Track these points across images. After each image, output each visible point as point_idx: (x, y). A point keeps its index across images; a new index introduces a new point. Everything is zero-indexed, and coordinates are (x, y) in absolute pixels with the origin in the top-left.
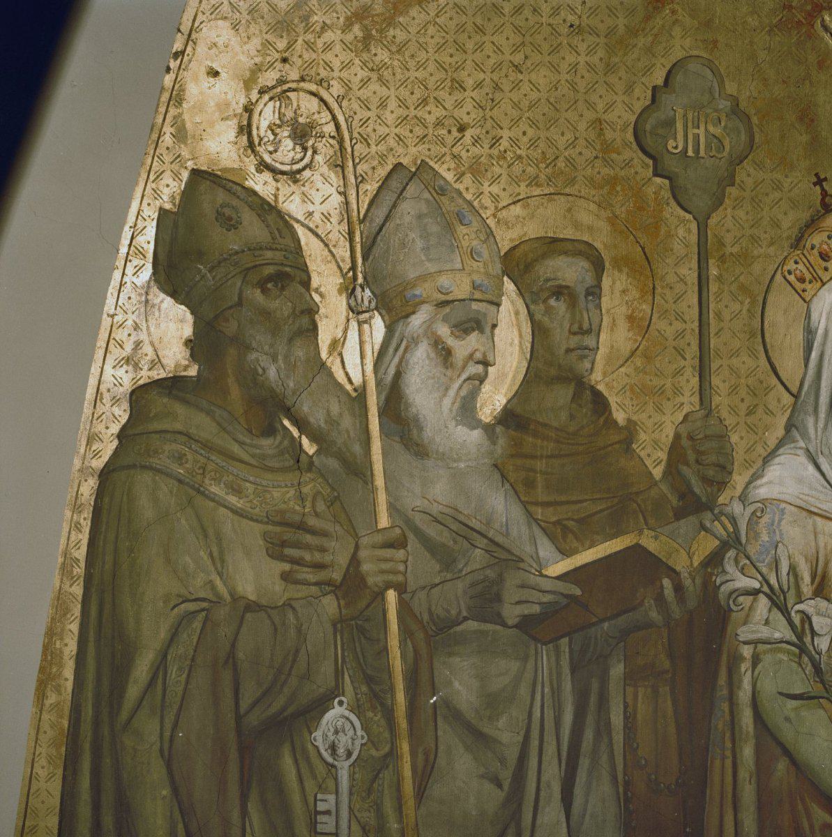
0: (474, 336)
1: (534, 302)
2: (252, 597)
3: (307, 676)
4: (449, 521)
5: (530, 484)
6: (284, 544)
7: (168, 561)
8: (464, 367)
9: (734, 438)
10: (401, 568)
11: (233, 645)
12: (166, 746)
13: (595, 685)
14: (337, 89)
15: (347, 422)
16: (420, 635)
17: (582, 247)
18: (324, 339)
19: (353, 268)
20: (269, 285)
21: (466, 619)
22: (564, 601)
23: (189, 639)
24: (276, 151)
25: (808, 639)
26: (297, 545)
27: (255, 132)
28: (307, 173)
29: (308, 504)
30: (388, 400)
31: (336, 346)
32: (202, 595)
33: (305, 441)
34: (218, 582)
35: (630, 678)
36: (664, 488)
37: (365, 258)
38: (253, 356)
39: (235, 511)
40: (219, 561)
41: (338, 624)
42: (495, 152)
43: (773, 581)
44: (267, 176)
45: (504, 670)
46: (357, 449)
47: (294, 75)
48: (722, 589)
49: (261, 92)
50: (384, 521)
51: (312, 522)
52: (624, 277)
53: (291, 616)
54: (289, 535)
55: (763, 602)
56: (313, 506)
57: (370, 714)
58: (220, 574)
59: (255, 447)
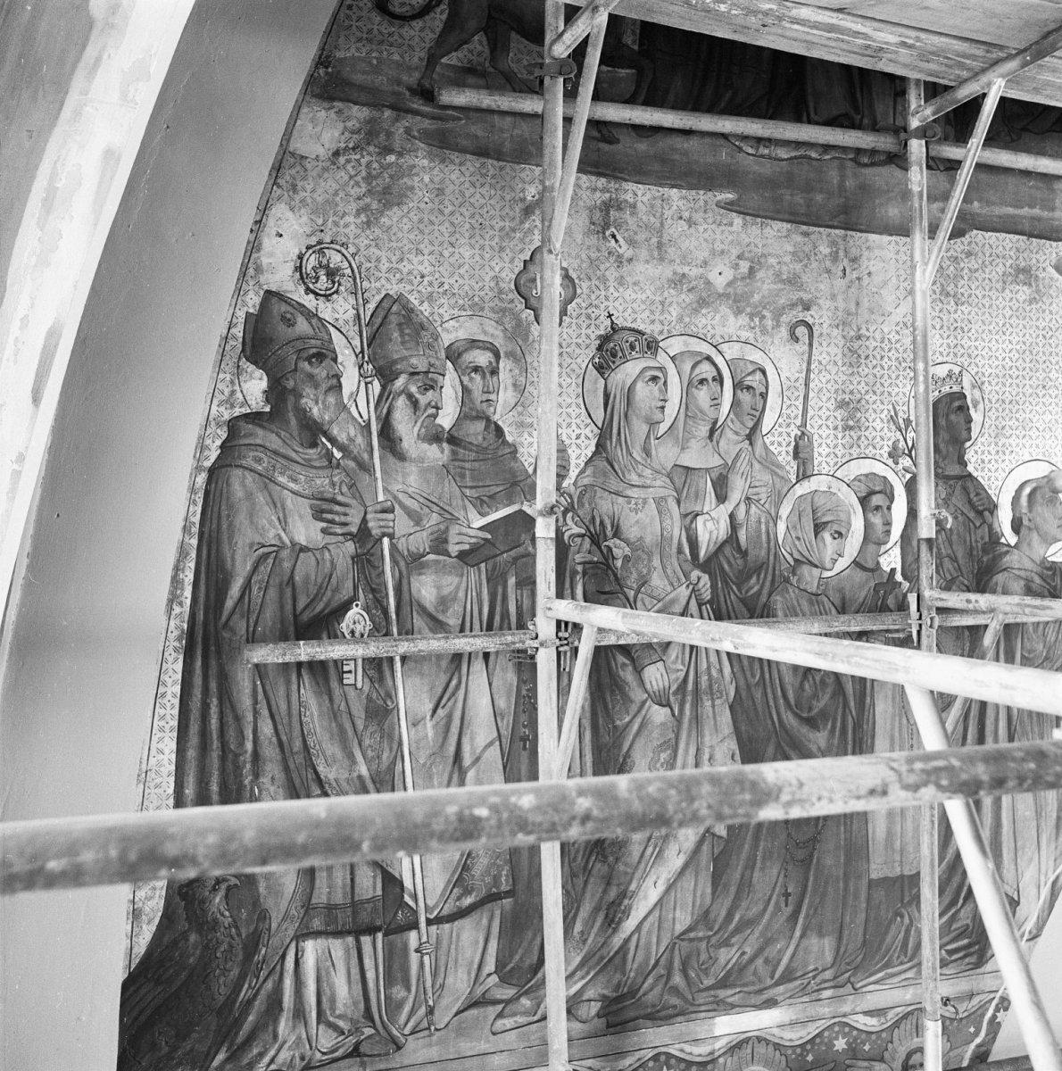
0: (431, 393)
1: (463, 374)
2: (304, 543)
3: (336, 590)
4: (417, 497)
5: (463, 476)
6: (323, 511)
7: (252, 522)
8: (425, 410)
9: (570, 451)
10: (391, 524)
11: (292, 572)
12: (250, 635)
13: (500, 590)
14: (352, 249)
15: (359, 440)
16: (402, 564)
17: (489, 346)
18: (346, 391)
19: (362, 352)
20: (314, 360)
21: (428, 553)
22: (483, 542)
24: (316, 282)
25: (610, 561)
26: (331, 512)
27: (304, 270)
28: (335, 296)
29: (337, 487)
30: (382, 428)
31: (354, 396)
32: (273, 542)
33: (335, 451)
34: (283, 534)
37: (369, 346)
38: (304, 401)
39: (293, 492)
40: (283, 522)
41: (356, 558)
42: (441, 290)
43: (592, 530)
44: (311, 296)
45: (450, 582)
46: (366, 456)
47: (328, 240)
49: (308, 248)
50: (381, 498)
51: (340, 498)
52: (510, 362)
53: (327, 554)
54: (325, 506)
55: (587, 540)
56: (340, 489)
57: (374, 611)
58: (284, 530)
59: (306, 454)
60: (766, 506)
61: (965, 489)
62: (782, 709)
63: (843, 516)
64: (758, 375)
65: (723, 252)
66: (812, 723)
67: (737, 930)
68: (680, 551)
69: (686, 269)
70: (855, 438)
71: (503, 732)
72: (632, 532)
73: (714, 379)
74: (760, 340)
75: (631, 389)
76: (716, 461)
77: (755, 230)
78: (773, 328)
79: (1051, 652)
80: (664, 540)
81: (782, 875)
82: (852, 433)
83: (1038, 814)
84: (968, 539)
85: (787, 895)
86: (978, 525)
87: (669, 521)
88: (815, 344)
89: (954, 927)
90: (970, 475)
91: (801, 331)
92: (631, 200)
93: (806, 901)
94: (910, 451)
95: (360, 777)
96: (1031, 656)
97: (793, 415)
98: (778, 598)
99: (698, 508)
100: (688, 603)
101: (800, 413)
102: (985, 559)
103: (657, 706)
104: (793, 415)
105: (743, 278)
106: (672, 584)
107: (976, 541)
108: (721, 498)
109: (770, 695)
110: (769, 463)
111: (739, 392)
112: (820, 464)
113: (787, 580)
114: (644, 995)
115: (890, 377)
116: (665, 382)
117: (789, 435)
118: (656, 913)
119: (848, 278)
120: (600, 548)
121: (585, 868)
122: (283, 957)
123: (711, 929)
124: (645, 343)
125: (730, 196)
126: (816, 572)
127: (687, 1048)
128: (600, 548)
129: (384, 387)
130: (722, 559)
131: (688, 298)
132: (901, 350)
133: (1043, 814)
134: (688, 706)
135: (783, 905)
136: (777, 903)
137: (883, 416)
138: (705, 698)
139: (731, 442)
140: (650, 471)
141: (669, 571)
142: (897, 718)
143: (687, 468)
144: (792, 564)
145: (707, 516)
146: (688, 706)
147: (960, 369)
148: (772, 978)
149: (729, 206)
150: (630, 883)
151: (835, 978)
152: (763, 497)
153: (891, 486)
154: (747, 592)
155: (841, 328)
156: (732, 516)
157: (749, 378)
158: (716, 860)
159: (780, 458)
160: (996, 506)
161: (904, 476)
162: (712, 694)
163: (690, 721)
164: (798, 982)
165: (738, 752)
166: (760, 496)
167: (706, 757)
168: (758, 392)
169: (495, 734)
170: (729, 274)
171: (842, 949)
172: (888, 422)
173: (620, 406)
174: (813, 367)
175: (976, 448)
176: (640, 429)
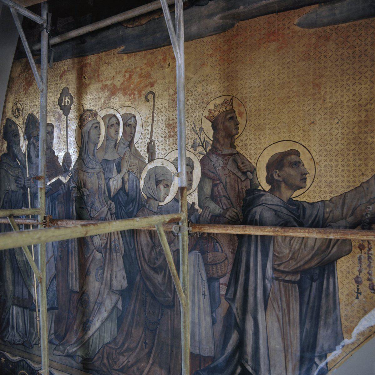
9: (72, 157)
14: (22, 102)
18: (21, 145)
23: (6, 197)
31: (22, 145)
33: (19, 162)
35: (58, 203)
36: (62, 167)
43: (77, 184)
47: (17, 101)
50: (28, 176)
60: (136, 174)
61: (235, 161)
62: (143, 262)
63: (169, 177)
64: (133, 119)
65: (120, 72)
67: (127, 350)
68: (104, 193)
69: (106, 83)
70: (175, 140)
71: (55, 254)
72: (89, 186)
73: (116, 124)
74: (133, 104)
75: (89, 132)
76: (116, 157)
77: (132, 59)
78: (138, 98)
79: (296, 256)
80: (99, 188)
81: (143, 335)
82: (173, 138)
84: (237, 188)
85: (146, 344)
86: (243, 179)
87: (101, 181)
88: (156, 100)
90: (238, 153)
91: (150, 96)
92: (90, 62)
93: (154, 349)
94: (203, 144)
95: (24, 260)
96: (281, 255)
97: (147, 134)
98: (140, 213)
99: (110, 176)
100: (107, 213)
101: (150, 132)
102: (248, 198)
103: (97, 252)
104: (147, 134)
105: (127, 80)
106: (102, 205)
107: (242, 189)
108: (119, 172)
109: (137, 255)
110: (137, 155)
111: (125, 127)
112: (158, 154)
113: (144, 206)
114: (95, 362)
115: (192, 109)
116: (100, 128)
117: (145, 142)
118: (98, 332)
119: (171, 67)
120: (80, 191)
121: (77, 306)
122: (10, 309)
123: (117, 346)
124: (93, 114)
125: (122, 48)
126: (156, 202)
128: (80, 191)
129: (28, 142)
130: (119, 196)
131: (107, 94)
132: (197, 95)
133: (290, 351)
134: (108, 254)
136: (142, 346)
137: (188, 128)
138: (113, 252)
139: (122, 148)
140: (95, 162)
141: (101, 201)
142: (196, 277)
143: (107, 160)
144: (146, 198)
145: (114, 179)
146: (108, 254)
147: (231, 97)
149: (123, 52)
150: (90, 318)
152: (135, 170)
153: (193, 162)
154: (128, 210)
155: (167, 91)
156: (123, 179)
157: (129, 121)
158: (118, 318)
159: (141, 153)
160: (255, 169)
161: (199, 156)
162: (116, 250)
163: (108, 261)
165: (125, 276)
166: (133, 170)
167: (114, 276)
168: (132, 126)
170: (122, 80)
172: (191, 131)
173: (86, 139)
174: (155, 111)
175: (242, 138)
176: (91, 146)
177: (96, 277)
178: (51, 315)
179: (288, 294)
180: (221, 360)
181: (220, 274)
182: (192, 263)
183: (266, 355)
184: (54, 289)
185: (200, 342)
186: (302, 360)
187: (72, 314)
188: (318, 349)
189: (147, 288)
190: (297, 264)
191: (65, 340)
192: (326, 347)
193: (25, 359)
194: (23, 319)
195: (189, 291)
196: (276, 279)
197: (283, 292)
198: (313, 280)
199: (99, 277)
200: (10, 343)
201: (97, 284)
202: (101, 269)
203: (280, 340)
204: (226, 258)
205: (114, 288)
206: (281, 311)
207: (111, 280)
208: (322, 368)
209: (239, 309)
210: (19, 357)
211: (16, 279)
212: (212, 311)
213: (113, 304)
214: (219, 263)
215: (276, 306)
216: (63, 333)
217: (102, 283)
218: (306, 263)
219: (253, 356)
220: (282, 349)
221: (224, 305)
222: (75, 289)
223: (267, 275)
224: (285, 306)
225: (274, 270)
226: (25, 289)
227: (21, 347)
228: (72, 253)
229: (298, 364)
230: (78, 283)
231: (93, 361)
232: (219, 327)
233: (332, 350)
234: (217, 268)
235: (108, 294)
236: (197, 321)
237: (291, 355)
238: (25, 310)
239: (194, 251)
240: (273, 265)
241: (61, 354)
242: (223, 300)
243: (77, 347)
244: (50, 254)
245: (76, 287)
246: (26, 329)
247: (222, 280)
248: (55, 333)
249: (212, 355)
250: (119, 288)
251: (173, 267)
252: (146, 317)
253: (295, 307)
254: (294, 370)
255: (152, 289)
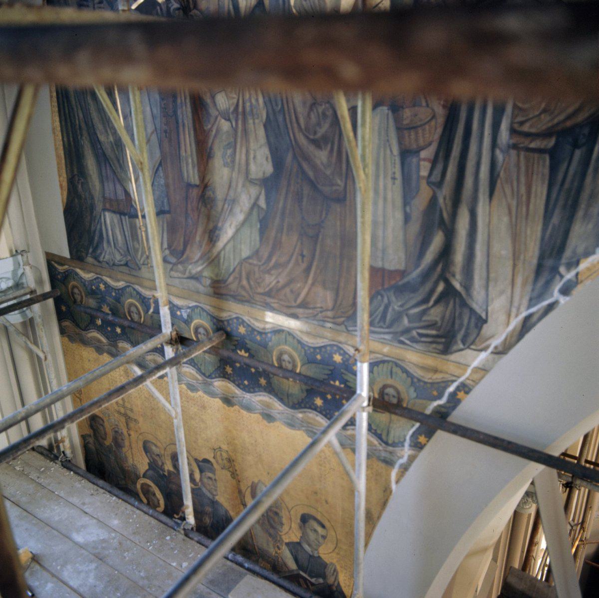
48: (172, 9)
55: (181, 11)
62: (296, 130)
66: (317, 144)
67: (275, 267)
71: (158, 127)
83: (515, 257)
85: (303, 256)
89: (424, 318)
93: (315, 264)
118: (231, 243)
121: (197, 208)
123: (260, 261)
127: (252, 320)
134: (240, 122)
135: (300, 261)
146: (240, 122)
148: (295, 301)
151: (334, 318)
158: (261, 221)
163: (242, 130)
164: (311, 311)
167: (252, 156)
169: (154, 128)
171: (339, 302)
177: (223, 161)
178: (161, 223)
179: (530, 170)
180: (415, 274)
181: (421, 142)
182: (376, 128)
183: (484, 266)
184: (162, 183)
185: (384, 251)
186: (539, 269)
187: (191, 218)
188: (568, 253)
189: (303, 172)
190: (553, 119)
191: (185, 256)
192: (580, 250)
193: (132, 285)
194: (122, 230)
195: (371, 169)
196: (515, 147)
197: (523, 169)
198: (576, 146)
199: (229, 160)
200: (107, 263)
201: (226, 171)
202: (230, 148)
203: (508, 242)
204: (434, 117)
205: (253, 176)
206: (515, 197)
207: (247, 164)
208: (569, 281)
209: (448, 198)
210: (123, 283)
211: (104, 171)
212: (406, 203)
213: (252, 201)
214: (421, 126)
215: (508, 191)
216: (181, 247)
217: (233, 170)
218: (569, 118)
219: (464, 267)
220: (511, 255)
221: (425, 192)
222: (193, 181)
223: (499, 142)
224: (523, 190)
225: (513, 131)
226: (118, 187)
227: (124, 269)
228: (184, 125)
229: (532, 276)
230: (196, 171)
231: (228, 282)
232: (415, 227)
233: (588, 254)
234: (417, 134)
235: (244, 186)
236: (381, 219)
237: (524, 263)
238: (123, 217)
239: (381, 108)
240: (512, 123)
241: (180, 275)
242: (424, 185)
243: (202, 264)
244: (150, 128)
245: (194, 177)
246: (127, 244)
247: (423, 154)
248: (169, 247)
249: (401, 267)
250: (260, 175)
251: (349, 126)
252: (303, 218)
253: (540, 190)
254: (524, 284)
255: (311, 174)
